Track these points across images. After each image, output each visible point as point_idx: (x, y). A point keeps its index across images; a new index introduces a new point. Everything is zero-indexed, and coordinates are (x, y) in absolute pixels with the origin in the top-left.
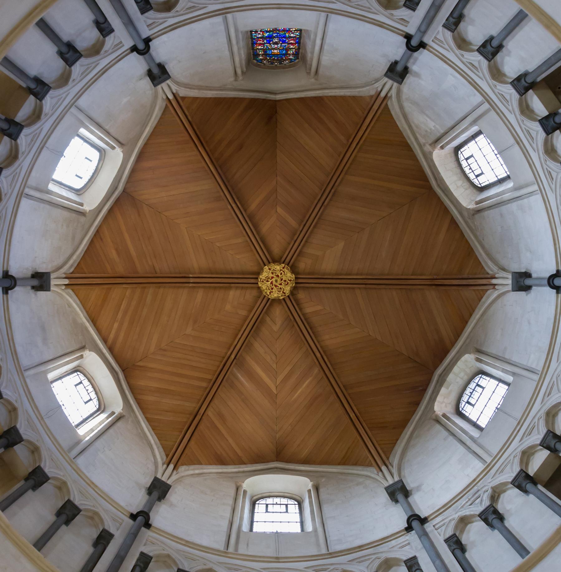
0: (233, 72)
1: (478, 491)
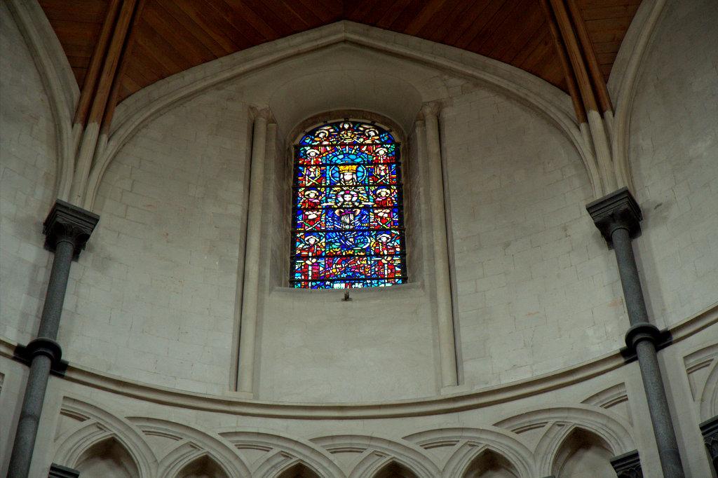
0: (447, 132)
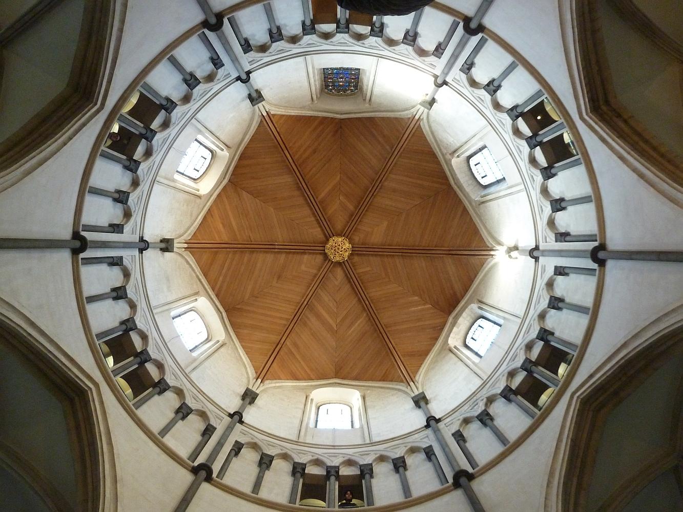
0: (310, 97)
1: (477, 400)
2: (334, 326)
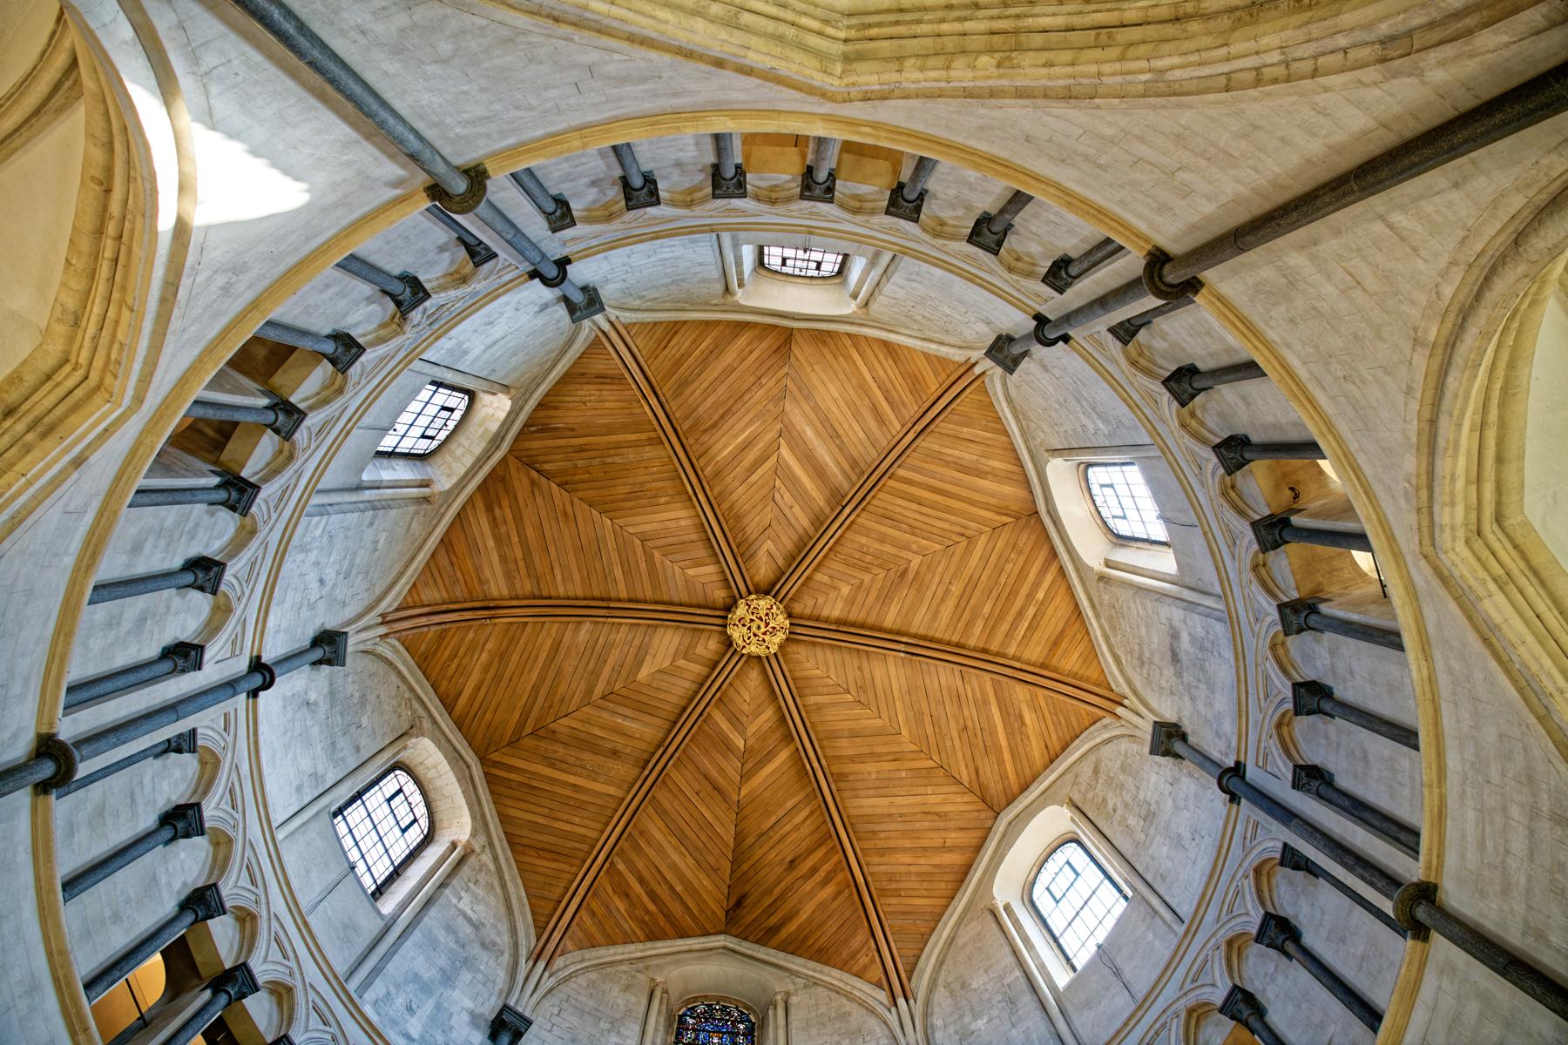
0: (792, 1011)
2: (785, 452)
